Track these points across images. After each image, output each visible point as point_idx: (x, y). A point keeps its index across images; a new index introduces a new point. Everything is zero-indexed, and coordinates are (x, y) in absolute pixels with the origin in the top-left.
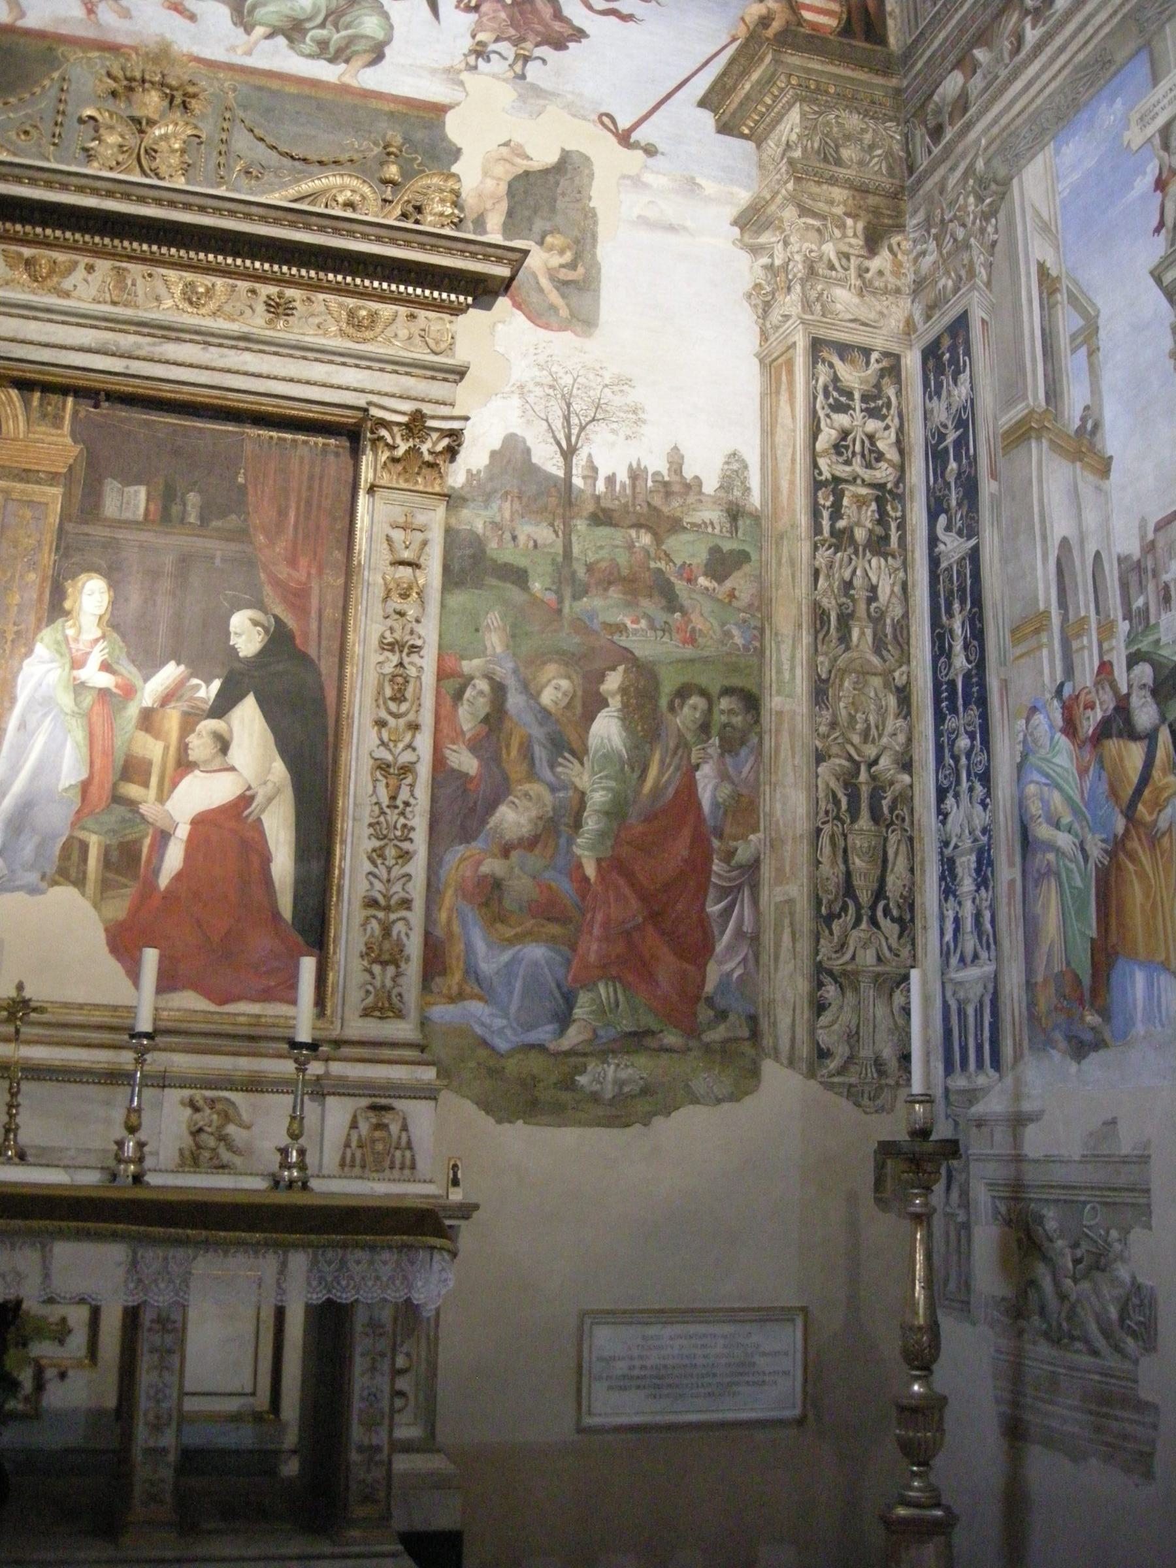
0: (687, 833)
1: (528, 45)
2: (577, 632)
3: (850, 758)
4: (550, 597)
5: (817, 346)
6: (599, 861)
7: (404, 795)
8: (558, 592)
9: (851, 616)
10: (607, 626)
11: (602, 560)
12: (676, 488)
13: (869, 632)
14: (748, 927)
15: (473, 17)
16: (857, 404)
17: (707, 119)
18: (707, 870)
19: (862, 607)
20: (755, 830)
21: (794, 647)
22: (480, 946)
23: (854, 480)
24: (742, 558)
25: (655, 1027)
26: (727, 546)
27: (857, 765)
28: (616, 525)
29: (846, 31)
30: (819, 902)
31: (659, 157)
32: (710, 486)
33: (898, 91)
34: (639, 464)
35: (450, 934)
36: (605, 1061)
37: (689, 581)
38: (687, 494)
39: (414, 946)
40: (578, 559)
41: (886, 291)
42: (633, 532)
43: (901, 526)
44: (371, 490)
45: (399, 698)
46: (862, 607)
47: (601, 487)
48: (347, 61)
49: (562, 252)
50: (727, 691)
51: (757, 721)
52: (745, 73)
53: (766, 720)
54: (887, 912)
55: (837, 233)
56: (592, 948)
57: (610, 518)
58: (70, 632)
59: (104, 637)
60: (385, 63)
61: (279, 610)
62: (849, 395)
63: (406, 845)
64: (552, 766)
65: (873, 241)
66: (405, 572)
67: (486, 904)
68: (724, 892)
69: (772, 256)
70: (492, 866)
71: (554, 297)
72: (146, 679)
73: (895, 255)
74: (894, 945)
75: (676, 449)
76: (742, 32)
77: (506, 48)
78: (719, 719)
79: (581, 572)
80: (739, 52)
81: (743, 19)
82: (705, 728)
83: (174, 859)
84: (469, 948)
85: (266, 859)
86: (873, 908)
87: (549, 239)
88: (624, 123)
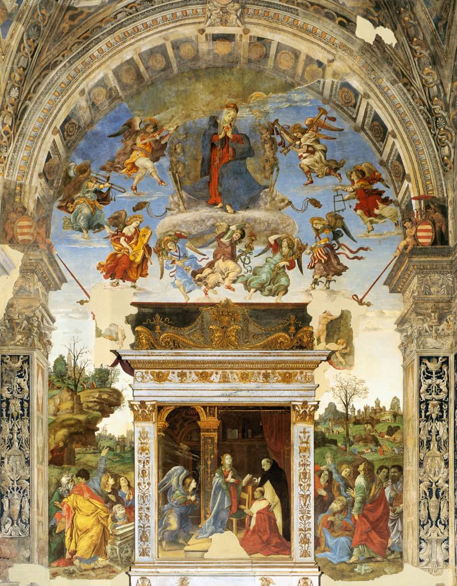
0: (382, 506)
1: (330, 276)
3: (430, 482)
4: (343, 446)
5: (421, 358)
6: (359, 515)
7: (308, 502)
8: (346, 445)
9: (431, 441)
10: (359, 452)
12: (378, 411)
13: (436, 445)
14: (400, 529)
15: (313, 270)
16: (434, 375)
17: (387, 288)
18: (388, 515)
19: (434, 438)
20: (402, 503)
21: (413, 452)
22: (329, 538)
23: (432, 400)
24: (398, 428)
25: (375, 556)
26: (393, 425)
27: (432, 483)
28: (361, 424)
29: (434, 243)
30: (420, 521)
31: (371, 306)
32: (388, 409)
33: (452, 261)
35: (321, 536)
36: (362, 565)
39: (312, 540)
41: (445, 336)
42: (366, 425)
43: (447, 412)
44: (294, 423)
45: (305, 478)
46: (434, 438)
47: (356, 414)
48: (277, 295)
49: (343, 344)
50: (393, 467)
51: (402, 474)
52: (399, 269)
53: (404, 473)
54: (440, 522)
55: (429, 319)
56: (357, 537)
58: (223, 469)
59: (231, 470)
60: (288, 292)
61: (273, 458)
62: (431, 373)
63: (309, 515)
64: (345, 492)
65: (441, 319)
66: (304, 445)
67: (329, 528)
68: (393, 520)
69: (407, 332)
70: (330, 519)
71: (341, 359)
72: (243, 479)
73: (448, 322)
74: (442, 531)
75: (377, 399)
76: (398, 253)
77: (324, 279)
78: (391, 474)
79: (351, 439)
80: (397, 261)
81: (398, 248)
82: (387, 477)
83: (253, 522)
84: (326, 539)
85: (275, 520)
86: (436, 522)
87: (339, 341)
88: (360, 297)
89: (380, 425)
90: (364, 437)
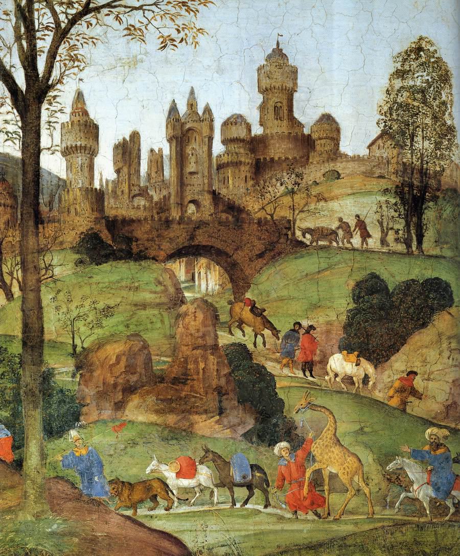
2: (55, 508)
10: (121, 486)
11: (112, 338)
12: (279, 150)
28: (140, 257)
34: (192, 105)
37: (308, 366)
38: (305, 160)
40: (55, 345)
42: (179, 269)
57: (129, 240)
89: (306, 264)
90: (162, 363)
